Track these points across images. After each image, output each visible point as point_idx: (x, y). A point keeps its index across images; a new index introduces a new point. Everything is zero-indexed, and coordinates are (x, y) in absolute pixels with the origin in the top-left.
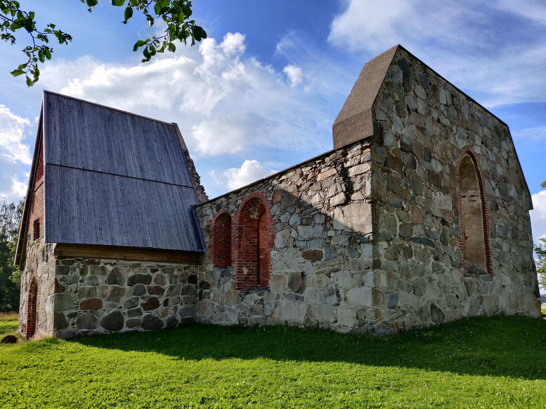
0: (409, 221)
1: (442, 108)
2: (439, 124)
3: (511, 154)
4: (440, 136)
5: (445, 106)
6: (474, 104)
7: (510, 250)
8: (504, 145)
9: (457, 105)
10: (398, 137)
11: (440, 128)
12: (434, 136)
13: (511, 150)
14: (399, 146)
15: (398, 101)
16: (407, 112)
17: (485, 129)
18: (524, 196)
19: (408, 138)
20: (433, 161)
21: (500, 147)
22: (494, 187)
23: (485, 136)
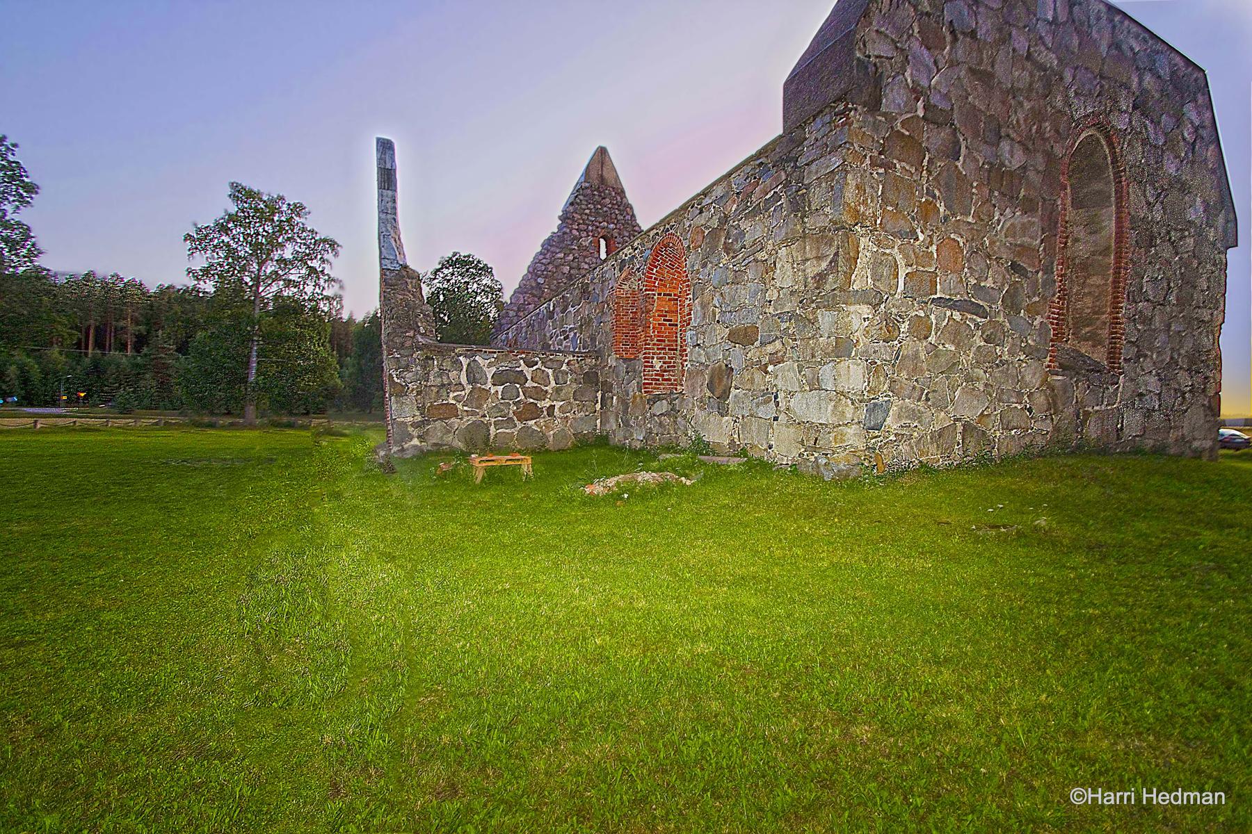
0: (930, 266)
1: (1042, 29)
2: (1028, 65)
3: (1204, 133)
4: (1030, 88)
5: (1050, 24)
6: (1126, 23)
7: (1169, 326)
8: (1190, 112)
9: (1082, 24)
10: (917, 92)
11: (1032, 75)
12: (1013, 92)
13: (1207, 123)
14: (921, 113)
15: (928, 14)
16: (949, 38)
17: (1148, 78)
18: (1221, 220)
19: (946, 97)
20: (1005, 146)
21: (1179, 120)
22: (1151, 200)
23: (1144, 92)
